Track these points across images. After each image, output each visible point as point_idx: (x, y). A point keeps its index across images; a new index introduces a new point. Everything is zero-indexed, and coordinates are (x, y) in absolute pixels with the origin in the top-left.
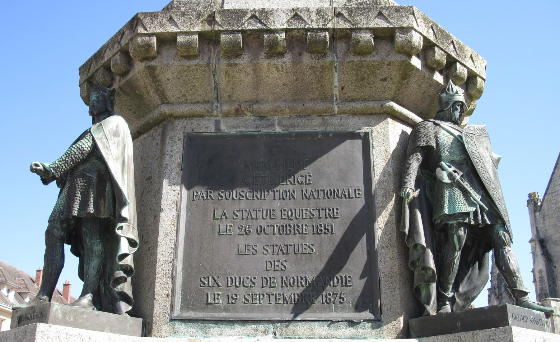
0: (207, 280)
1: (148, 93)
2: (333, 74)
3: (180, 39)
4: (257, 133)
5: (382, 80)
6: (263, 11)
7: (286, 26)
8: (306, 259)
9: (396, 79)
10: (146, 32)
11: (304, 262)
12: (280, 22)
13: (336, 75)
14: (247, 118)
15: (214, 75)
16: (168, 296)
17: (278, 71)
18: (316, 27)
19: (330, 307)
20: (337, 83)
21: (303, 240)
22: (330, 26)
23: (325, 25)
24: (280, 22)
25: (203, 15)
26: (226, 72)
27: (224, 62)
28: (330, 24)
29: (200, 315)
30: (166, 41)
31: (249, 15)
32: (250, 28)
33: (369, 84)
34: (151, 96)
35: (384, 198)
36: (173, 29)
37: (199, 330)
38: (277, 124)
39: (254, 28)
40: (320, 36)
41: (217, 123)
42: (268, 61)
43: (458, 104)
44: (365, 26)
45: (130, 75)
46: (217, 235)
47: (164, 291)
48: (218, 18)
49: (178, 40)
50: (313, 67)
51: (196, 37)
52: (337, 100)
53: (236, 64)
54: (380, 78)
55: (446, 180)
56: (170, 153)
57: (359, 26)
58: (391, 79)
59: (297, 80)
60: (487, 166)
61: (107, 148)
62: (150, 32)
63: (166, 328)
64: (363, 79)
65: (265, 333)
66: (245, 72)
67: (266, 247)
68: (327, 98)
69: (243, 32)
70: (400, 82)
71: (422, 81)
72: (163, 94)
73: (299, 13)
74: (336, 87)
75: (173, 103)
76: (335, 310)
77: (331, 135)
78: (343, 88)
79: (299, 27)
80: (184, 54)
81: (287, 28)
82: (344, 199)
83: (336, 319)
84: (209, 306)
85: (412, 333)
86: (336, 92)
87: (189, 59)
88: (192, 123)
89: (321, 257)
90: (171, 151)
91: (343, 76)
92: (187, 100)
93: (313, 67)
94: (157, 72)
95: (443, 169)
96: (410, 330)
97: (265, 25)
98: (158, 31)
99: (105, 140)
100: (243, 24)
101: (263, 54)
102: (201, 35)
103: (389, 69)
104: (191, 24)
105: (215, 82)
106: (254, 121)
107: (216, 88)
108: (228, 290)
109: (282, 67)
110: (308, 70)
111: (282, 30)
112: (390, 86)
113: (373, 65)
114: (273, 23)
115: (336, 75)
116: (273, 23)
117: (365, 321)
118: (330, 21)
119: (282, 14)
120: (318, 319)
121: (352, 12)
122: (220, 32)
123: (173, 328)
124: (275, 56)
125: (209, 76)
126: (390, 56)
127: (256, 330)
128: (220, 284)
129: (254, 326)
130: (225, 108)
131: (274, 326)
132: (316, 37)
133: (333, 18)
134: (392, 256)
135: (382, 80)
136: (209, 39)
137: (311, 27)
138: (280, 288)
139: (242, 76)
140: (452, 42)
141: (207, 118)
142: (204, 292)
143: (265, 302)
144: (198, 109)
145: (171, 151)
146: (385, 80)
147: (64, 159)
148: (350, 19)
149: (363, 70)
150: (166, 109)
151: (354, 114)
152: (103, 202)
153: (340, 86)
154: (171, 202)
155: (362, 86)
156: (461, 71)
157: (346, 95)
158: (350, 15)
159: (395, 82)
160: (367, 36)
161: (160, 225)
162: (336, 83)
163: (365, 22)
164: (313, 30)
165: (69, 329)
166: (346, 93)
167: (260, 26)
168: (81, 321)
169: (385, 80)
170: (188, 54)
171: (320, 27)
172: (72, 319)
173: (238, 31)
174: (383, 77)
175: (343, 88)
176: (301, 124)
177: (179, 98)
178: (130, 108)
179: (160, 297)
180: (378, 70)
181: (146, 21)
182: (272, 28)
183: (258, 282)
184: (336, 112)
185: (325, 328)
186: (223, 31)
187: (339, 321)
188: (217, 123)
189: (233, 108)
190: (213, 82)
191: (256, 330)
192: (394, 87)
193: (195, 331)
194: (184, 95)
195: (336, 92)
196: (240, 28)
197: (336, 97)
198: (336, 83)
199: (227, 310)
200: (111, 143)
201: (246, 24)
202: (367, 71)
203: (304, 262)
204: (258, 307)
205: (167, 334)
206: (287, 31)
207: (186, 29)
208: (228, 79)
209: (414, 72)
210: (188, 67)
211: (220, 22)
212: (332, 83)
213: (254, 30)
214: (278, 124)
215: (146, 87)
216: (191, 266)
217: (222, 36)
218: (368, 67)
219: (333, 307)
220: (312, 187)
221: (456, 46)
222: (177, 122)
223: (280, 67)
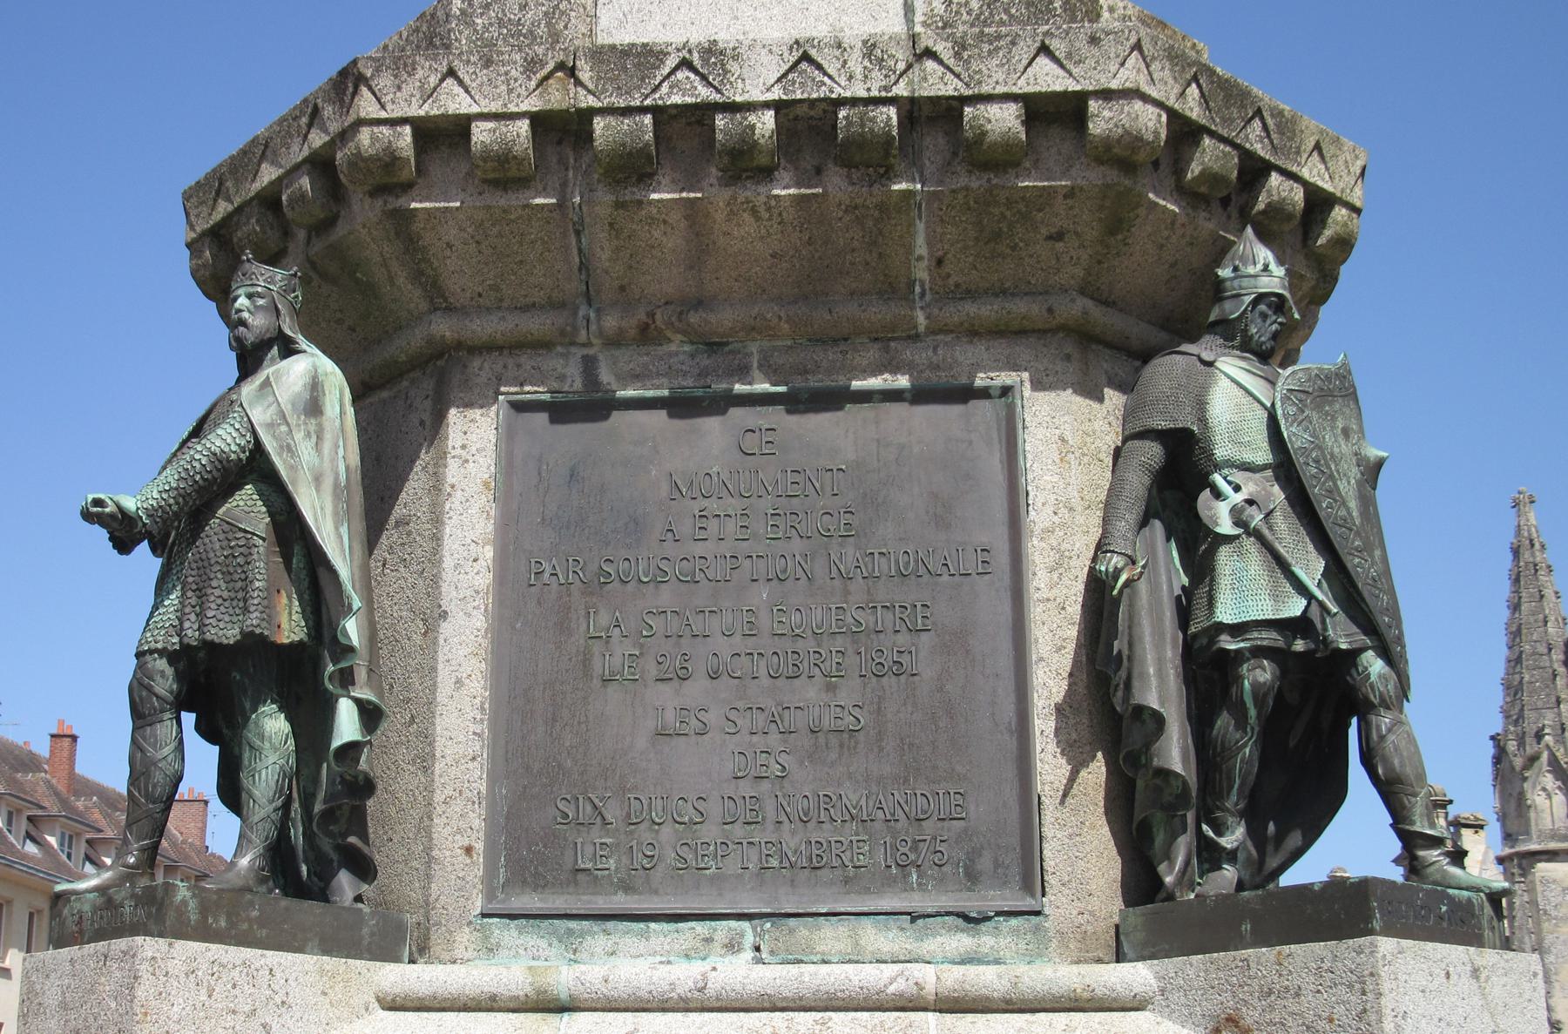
0: (573, 807)
1: (391, 279)
2: (911, 224)
3: (481, 134)
4: (700, 393)
5: (1050, 238)
6: (711, 50)
7: (776, 94)
8: (841, 746)
10: (383, 115)
11: (833, 756)
12: (758, 82)
13: (921, 226)
14: (673, 347)
15: (578, 233)
16: (469, 850)
17: (758, 219)
18: (864, 94)
19: (906, 876)
21: (830, 695)
22: (901, 90)
23: (886, 88)
24: (758, 82)
25: (543, 64)
26: (611, 224)
27: (605, 197)
28: (902, 84)
29: (559, 903)
30: (442, 136)
31: (671, 62)
32: (677, 99)
33: (1014, 248)
34: (399, 288)
35: (1055, 576)
36: (456, 102)
37: (555, 942)
38: (755, 365)
39: (689, 100)
40: (873, 120)
41: (589, 365)
42: (727, 193)
43: (1267, 300)
44: (1000, 89)
45: (340, 230)
46: (596, 683)
47: (458, 837)
48: (585, 75)
49: (474, 139)
50: (856, 207)
51: (523, 126)
52: (923, 294)
53: (640, 203)
54: (1044, 231)
55: (1226, 527)
56: (458, 451)
57: (986, 89)
58: (1076, 233)
59: (810, 242)
60: (1342, 485)
61: (289, 448)
62: (394, 115)
63: (465, 938)
64: (997, 236)
65: (733, 947)
66: (665, 222)
67: (733, 715)
68: (896, 289)
69: (656, 110)
72: (435, 284)
73: (813, 53)
74: (920, 258)
75: (464, 307)
76: (919, 884)
77: (907, 395)
78: (940, 262)
79: (815, 96)
80: (491, 176)
81: (780, 100)
82: (945, 578)
83: (921, 911)
84: (580, 876)
85: (1126, 947)
86: (921, 273)
87: (505, 190)
88: (519, 366)
89: (881, 740)
90: (464, 447)
91: (939, 230)
92: (501, 300)
93: (856, 207)
94: (417, 226)
95: (1218, 495)
96: (1122, 938)
97: (718, 91)
98: (416, 110)
99: (284, 428)
100: (657, 88)
101: (714, 170)
102: (541, 122)
103: (1071, 208)
104: (510, 91)
105: (580, 251)
106: (692, 356)
107: (583, 266)
108: (631, 832)
109: (769, 209)
110: (841, 214)
111: (766, 105)
112: (1073, 253)
113: (1023, 198)
114: (740, 85)
115: (921, 226)
116: (740, 85)
117: (998, 914)
118: (901, 75)
119: (765, 58)
120: (872, 909)
121: (964, 48)
122: (591, 112)
123: (487, 938)
124: (748, 178)
125: (565, 235)
126: (1073, 172)
127: (708, 940)
128: (609, 818)
129: (701, 928)
130: (611, 322)
131: (754, 929)
132: (863, 125)
133: (909, 67)
134: (1074, 736)
135: (1050, 238)
136: (561, 131)
137: (848, 94)
138: (770, 826)
139: (657, 234)
140: (1258, 113)
141: (559, 349)
142: (566, 839)
143: (732, 866)
144: (536, 324)
145: (464, 447)
146: (1059, 236)
147: (174, 485)
148: (957, 69)
149: (996, 211)
150: (443, 328)
151: (973, 332)
152: (285, 600)
153: (931, 254)
154: (469, 592)
156: (1284, 194)
157: (951, 281)
158: (957, 55)
160: (1004, 119)
161: (441, 658)
162: (921, 248)
163: (1000, 76)
164: (854, 102)
165: (216, 950)
166: (949, 276)
167: (704, 93)
168: (245, 926)
169: (1059, 236)
170: (503, 173)
171: (875, 93)
172: (223, 924)
173: (643, 110)
174: (1053, 230)
175: (940, 262)
176: (825, 364)
177: (480, 295)
178: (339, 315)
179: (448, 853)
180: (1040, 210)
181: (384, 82)
182: (738, 99)
183: (714, 808)
184: (922, 329)
185: (891, 935)
186: (602, 111)
187: (929, 916)
188: (589, 365)
189: (634, 322)
190: (575, 251)
191: (708, 940)
193: (543, 943)
194: (495, 288)
195: (921, 273)
196: (648, 102)
197: (922, 286)
198: (921, 248)
199: (628, 888)
200: (299, 436)
201: (665, 88)
202: (1008, 213)
203: (833, 756)
204: (712, 878)
205: (470, 954)
206: (778, 106)
207: (495, 107)
208: (616, 242)
209: (1142, 211)
210: (505, 211)
211: (591, 86)
212: (909, 249)
213: (686, 107)
214: (760, 366)
215: (385, 264)
216: (528, 768)
217: (599, 124)
218: (1009, 203)
220: (857, 547)
221: (1270, 122)
222: (476, 363)
223: (762, 209)
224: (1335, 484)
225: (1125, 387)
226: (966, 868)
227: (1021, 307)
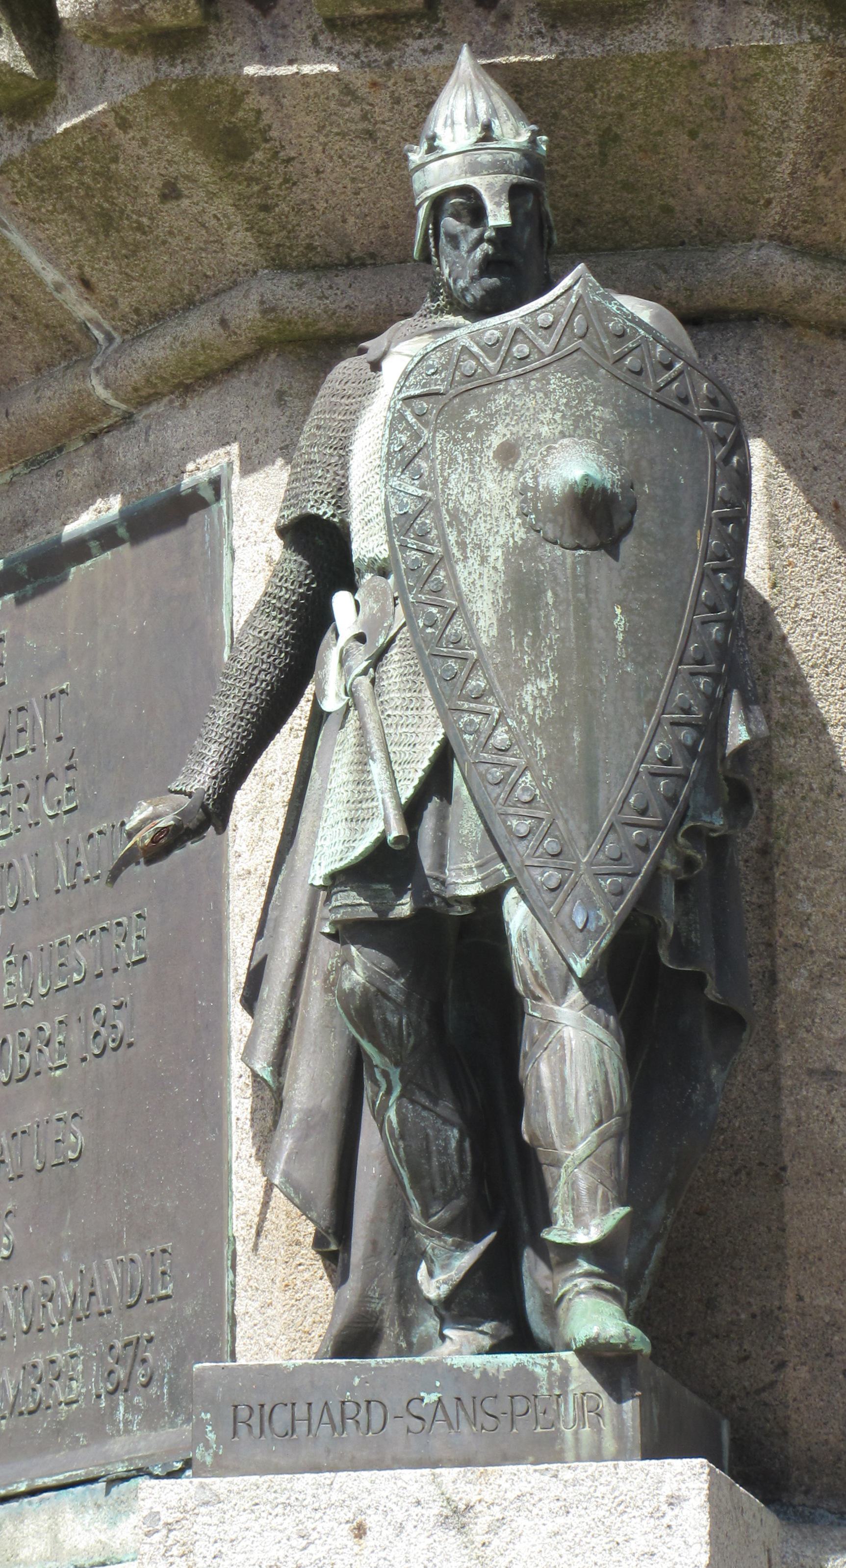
9: (204, 172)
13: (16, 238)
19: (114, 1408)
20: (49, 268)
33: (140, 228)
52: (110, 339)
58: (187, 177)
68: (71, 348)
70: (233, 177)
71: (354, 111)
74: (59, 287)
86: (84, 310)
103: (144, 142)
112: (212, 210)
153: (64, 272)
155: (135, 249)
157: (124, 305)
159: (212, 188)
169: (171, 192)
174: (159, 184)
175: (86, 284)
180: (115, 160)
192: (224, 204)
195: (84, 310)
197: (99, 326)
198: (50, 275)
212: (40, 283)
219: (122, 1409)
224: (453, 576)
225: (287, 450)
226: (171, 1385)
227: (199, 327)
